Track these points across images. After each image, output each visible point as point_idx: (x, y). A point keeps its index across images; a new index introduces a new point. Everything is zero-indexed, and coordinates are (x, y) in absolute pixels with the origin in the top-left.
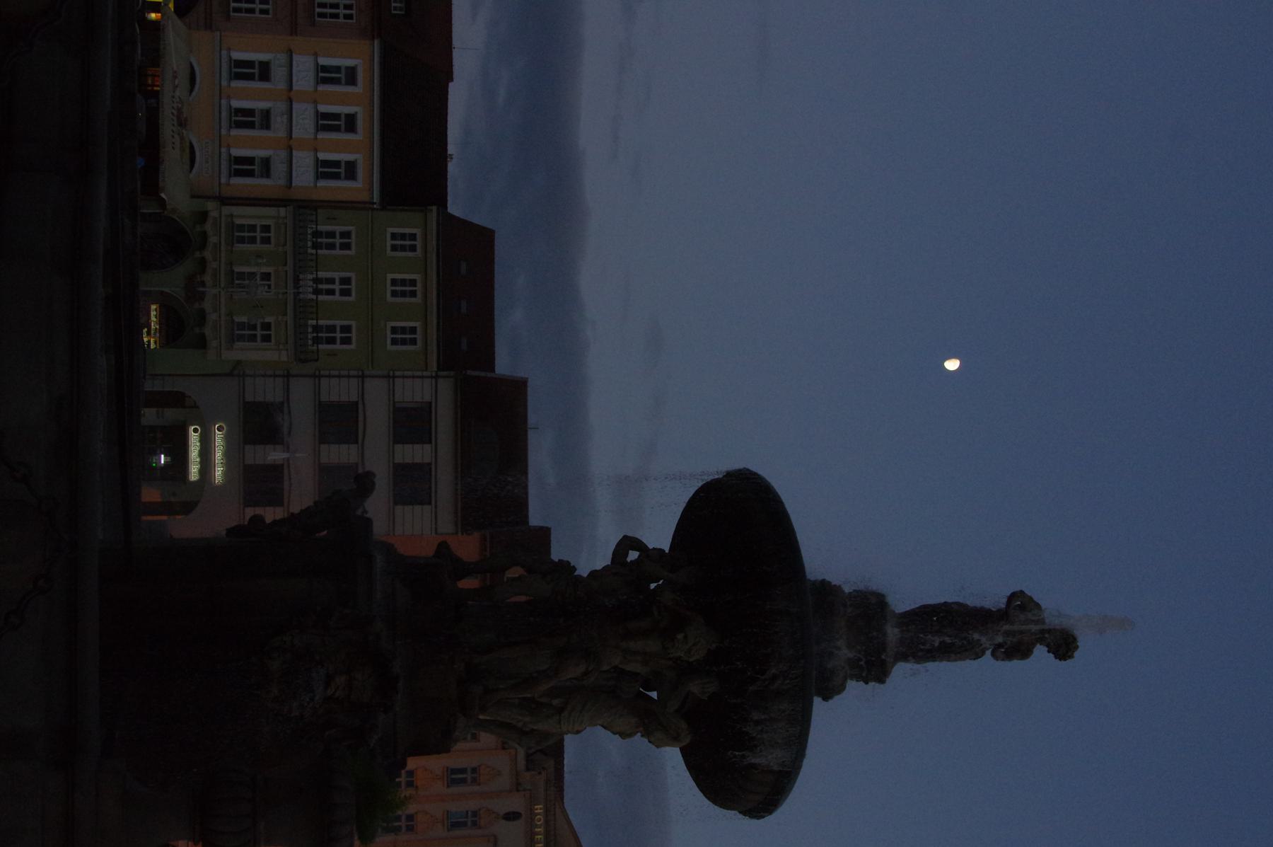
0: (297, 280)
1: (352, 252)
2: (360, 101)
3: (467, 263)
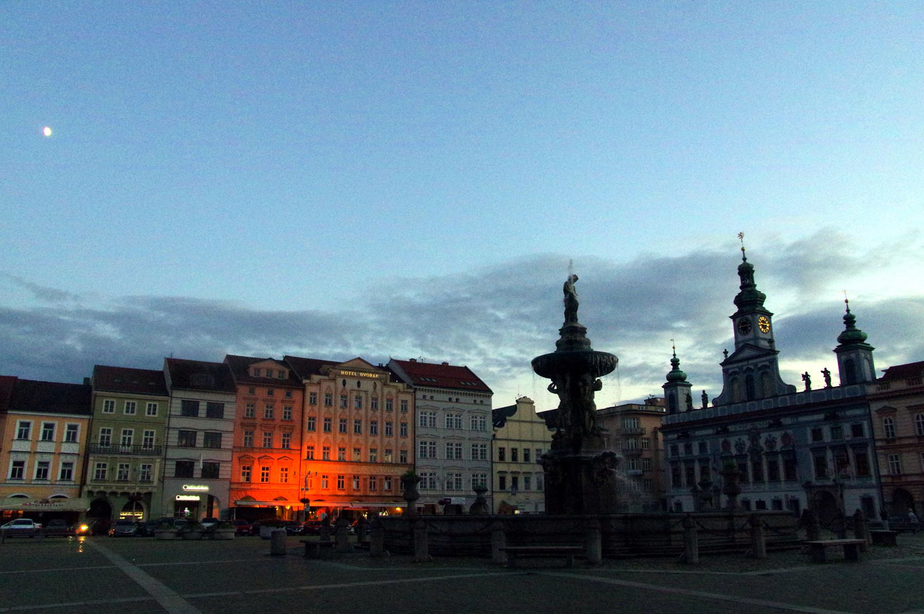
0: (122, 453)
1: (155, 431)
2: (37, 422)
3: (116, 379)
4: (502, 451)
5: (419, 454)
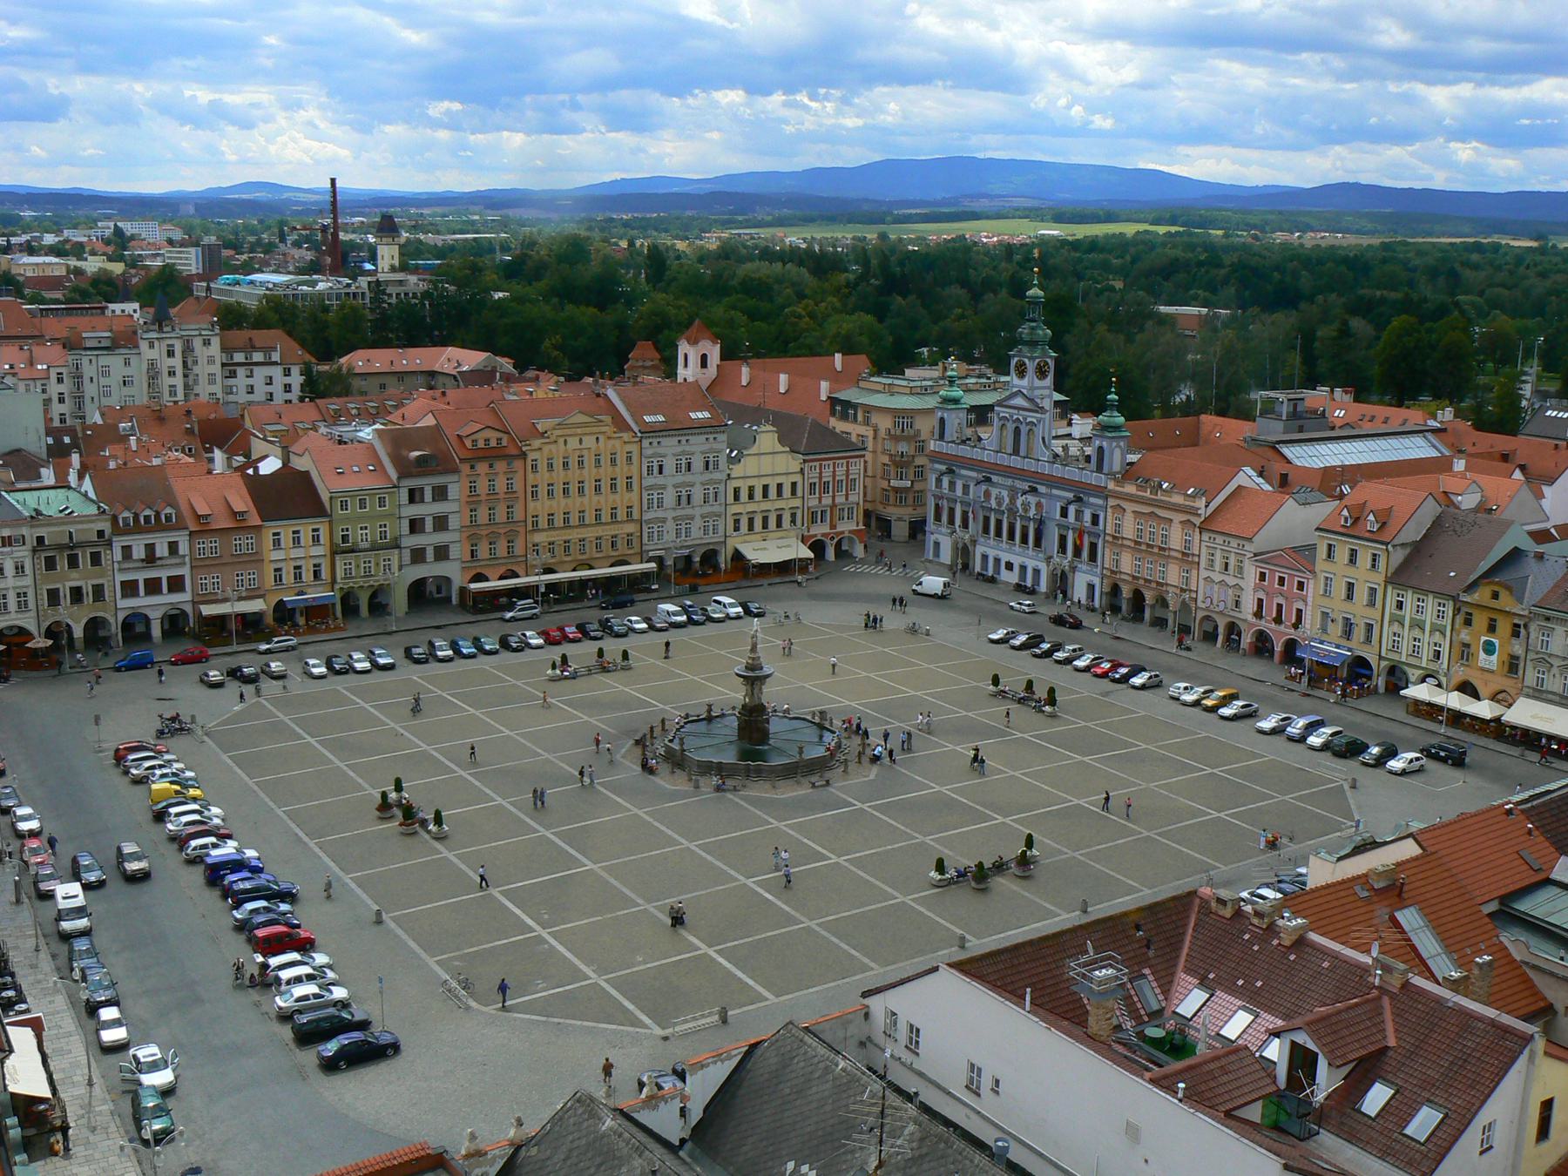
2: (286, 530)
4: (737, 491)
5: (645, 507)
